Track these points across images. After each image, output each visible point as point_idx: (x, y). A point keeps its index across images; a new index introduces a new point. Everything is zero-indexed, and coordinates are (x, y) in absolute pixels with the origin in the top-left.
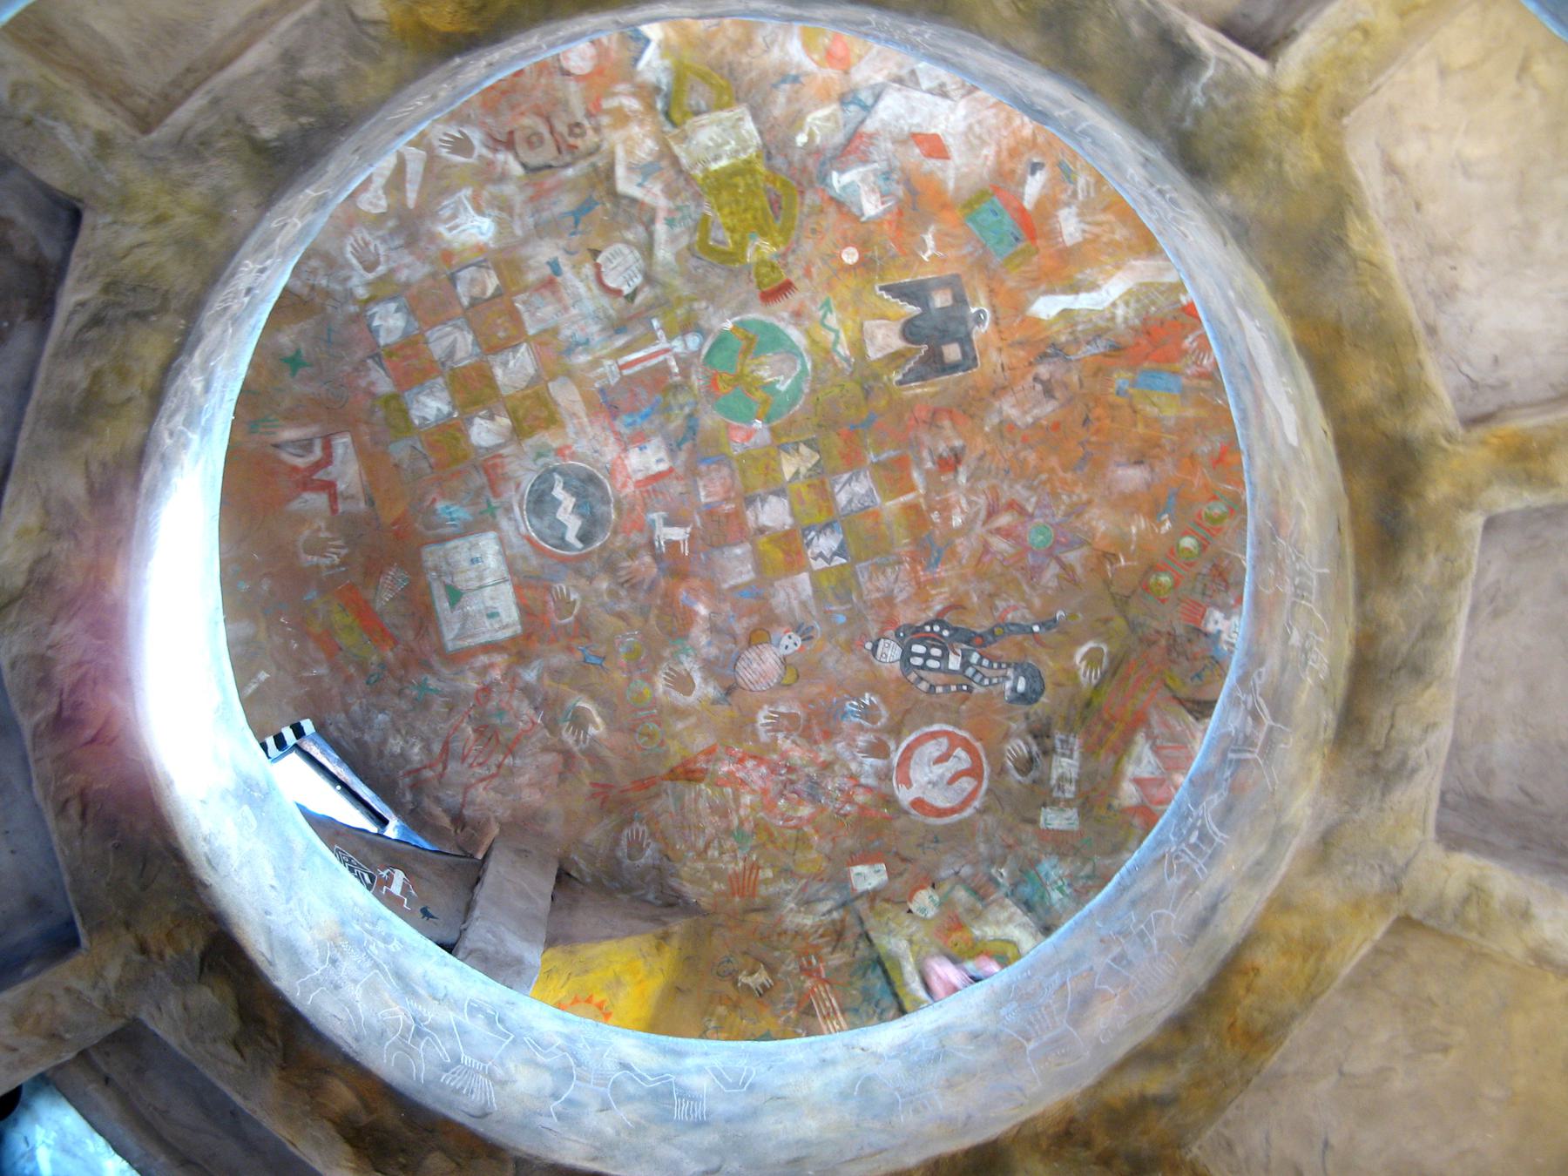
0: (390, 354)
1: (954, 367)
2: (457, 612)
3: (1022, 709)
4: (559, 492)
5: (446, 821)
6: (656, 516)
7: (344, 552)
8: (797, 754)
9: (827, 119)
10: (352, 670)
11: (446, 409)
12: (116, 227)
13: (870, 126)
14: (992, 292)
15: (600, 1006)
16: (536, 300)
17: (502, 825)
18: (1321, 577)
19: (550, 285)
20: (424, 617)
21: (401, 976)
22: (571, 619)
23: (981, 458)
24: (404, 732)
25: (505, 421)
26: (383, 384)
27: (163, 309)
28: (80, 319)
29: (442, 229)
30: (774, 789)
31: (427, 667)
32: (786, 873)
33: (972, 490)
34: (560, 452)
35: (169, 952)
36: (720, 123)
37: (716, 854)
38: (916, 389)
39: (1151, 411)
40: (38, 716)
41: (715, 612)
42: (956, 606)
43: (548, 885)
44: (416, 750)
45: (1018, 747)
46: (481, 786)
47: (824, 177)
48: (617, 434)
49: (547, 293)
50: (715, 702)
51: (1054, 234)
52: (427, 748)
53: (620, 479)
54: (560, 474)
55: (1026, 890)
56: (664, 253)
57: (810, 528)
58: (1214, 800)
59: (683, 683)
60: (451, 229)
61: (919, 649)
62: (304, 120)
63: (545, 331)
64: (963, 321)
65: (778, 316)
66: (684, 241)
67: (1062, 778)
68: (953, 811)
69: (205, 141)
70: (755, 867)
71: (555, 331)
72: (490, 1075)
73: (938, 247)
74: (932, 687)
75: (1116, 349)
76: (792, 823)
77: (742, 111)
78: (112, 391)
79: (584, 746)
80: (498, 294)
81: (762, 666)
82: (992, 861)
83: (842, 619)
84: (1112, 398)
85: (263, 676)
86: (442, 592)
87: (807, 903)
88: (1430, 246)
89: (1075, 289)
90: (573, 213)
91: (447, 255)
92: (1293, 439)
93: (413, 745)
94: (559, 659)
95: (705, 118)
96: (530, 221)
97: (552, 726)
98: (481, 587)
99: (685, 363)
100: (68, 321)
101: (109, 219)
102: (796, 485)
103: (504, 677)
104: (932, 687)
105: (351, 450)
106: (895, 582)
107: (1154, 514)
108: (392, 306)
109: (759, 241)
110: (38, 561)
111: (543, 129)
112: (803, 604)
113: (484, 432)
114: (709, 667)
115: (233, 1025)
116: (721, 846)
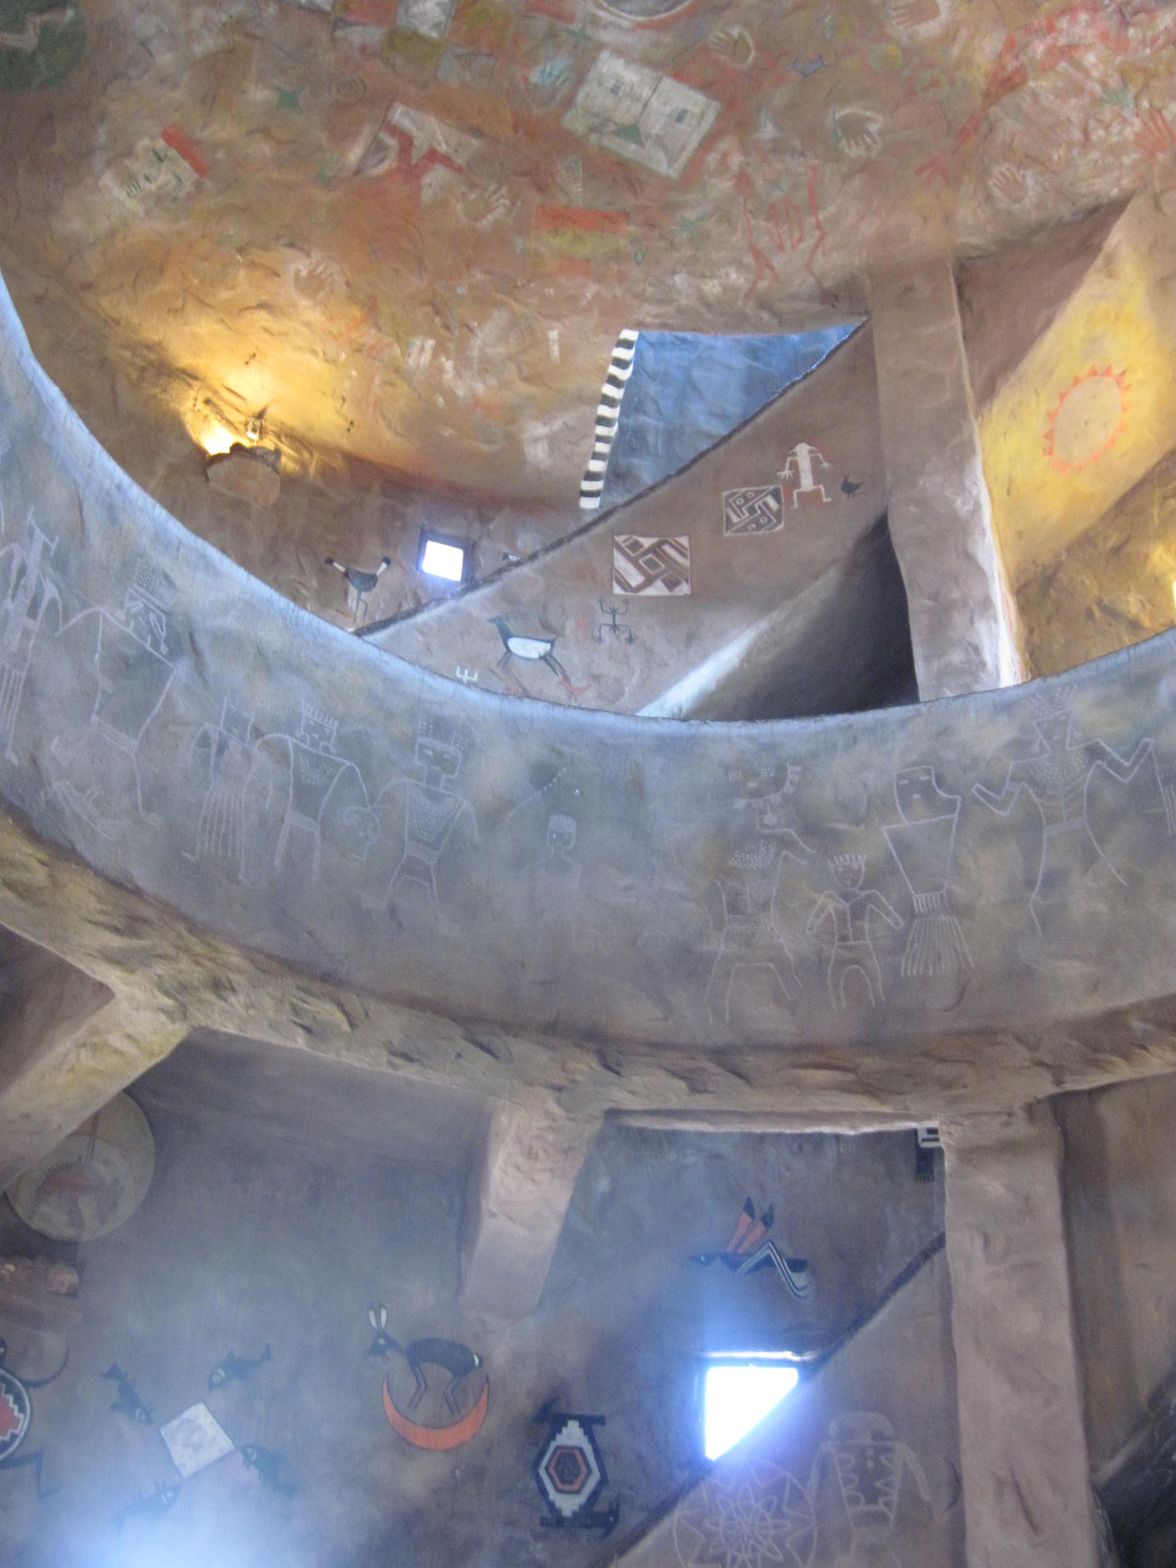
2: (648, 145)
7: (504, 190)
10: (614, 267)
15: (1093, 373)
22: (753, 53)
24: (709, 273)
30: (1110, 24)
31: (669, 207)
37: (1101, 132)
44: (734, 276)
46: (819, 257)
52: (741, 267)
76: (1160, 42)
79: (879, 147)
85: (553, 335)
86: (618, 140)
93: (727, 275)
98: (645, 105)
103: (746, 153)
105: (412, 112)
116: (1100, 121)
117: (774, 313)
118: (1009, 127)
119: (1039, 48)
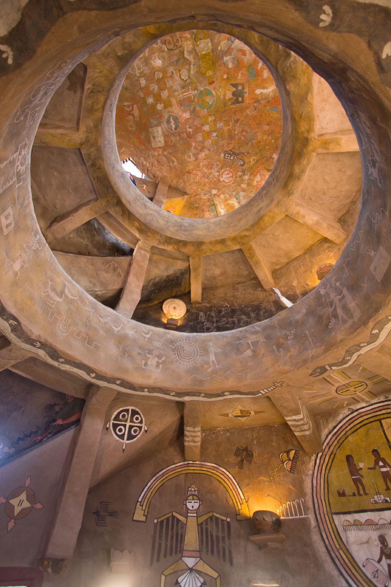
0: (143, 89)
1: (240, 102)
3: (241, 167)
4: (171, 120)
5: (152, 176)
6: (187, 126)
8: (206, 170)
9: (225, 43)
11: (153, 101)
12: (94, 72)
13: (233, 46)
14: (249, 87)
16: (169, 80)
17: (161, 178)
18: (288, 159)
19: (171, 77)
20: (149, 141)
21: (145, 206)
23: (242, 121)
25: (163, 105)
26: (142, 96)
27: (103, 91)
28: (89, 91)
29: (152, 62)
30: (202, 176)
31: (149, 150)
32: (202, 190)
33: (239, 127)
34: (172, 112)
35: (112, 202)
36: (204, 43)
38: (233, 106)
39: (272, 115)
40: (89, 164)
41: (196, 145)
42: (233, 148)
43: (167, 189)
45: (240, 174)
47: (223, 58)
48: (182, 110)
49: (171, 78)
50: (194, 161)
51: (262, 76)
53: (182, 118)
54: (172, 116)
55: (237, 196)
56: (192, 72)
57: (212, 131)
58: (265, 192)
59: (189, 157)
60: (154, 62)
61: (227, 155)
62: (126, 51)
63: (170, 87)
64: (243, 93)
65: (210, 88)
66: (196, 70)
67: (245, 179)
68: (228, 183)
69: (108, 55)
70: (198, 188)
71: (172, 87)
72: (157, 221)
73: (242, 76)
74: (228, 162)
75: (269, 101)
77: (209, 40)
78: (96, 107)
80: (162, 78)
81: (202, 155)
82: (233, 191)
83: (215, 148)
84: (266, 112)
87: (205, 195)
88: (322, 100)
89: (264, 88)
90: (176, 61)
91: (153, 68)
92: (290, 134)
94: (170, 151)
95: (202, 41)
96: (168, 62)
97: (169, 162)
99: (194, 96)
100: (87, 91)
101: (92, 70)
102: (210, 123)
104: (228, 162)
106: (225, 142)
107: (268, 135)
108: (143, 78)
109: (209, 71)
110: (86, 137)
111: (172, 41)
112: (210, 145)
113: (160, 107)
114: (194, 154)
115: (121, 213)
117: (148, 173)
118: (185, 177)
119: (195, 172)
